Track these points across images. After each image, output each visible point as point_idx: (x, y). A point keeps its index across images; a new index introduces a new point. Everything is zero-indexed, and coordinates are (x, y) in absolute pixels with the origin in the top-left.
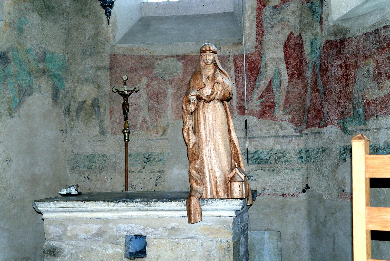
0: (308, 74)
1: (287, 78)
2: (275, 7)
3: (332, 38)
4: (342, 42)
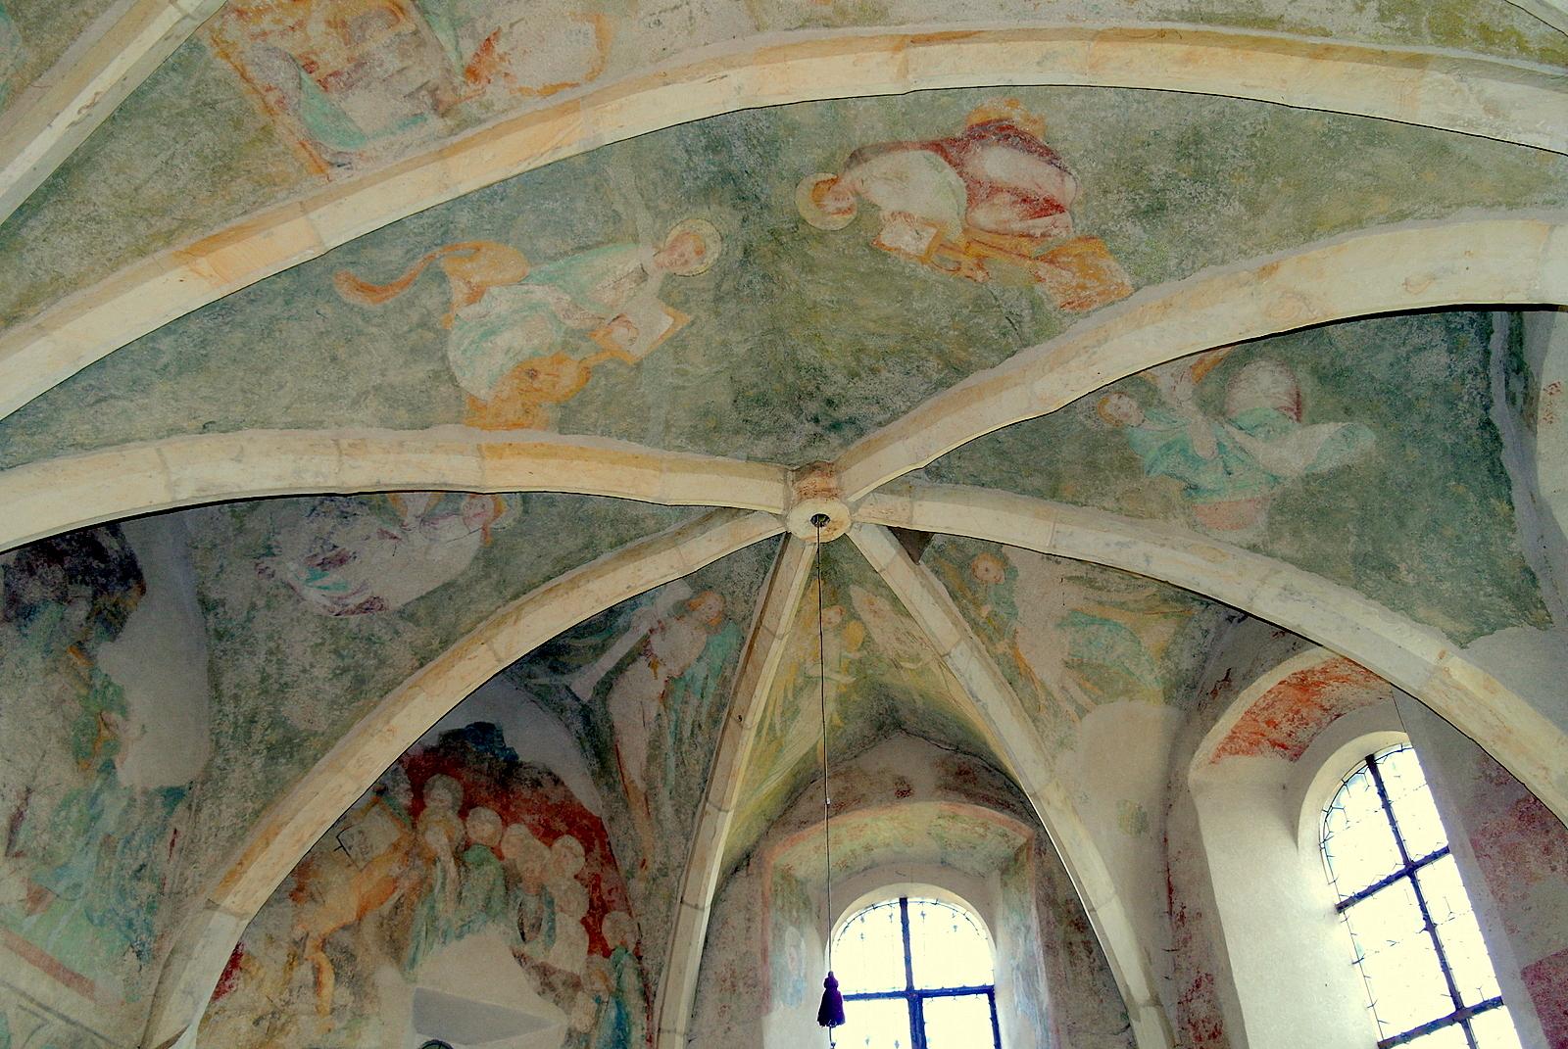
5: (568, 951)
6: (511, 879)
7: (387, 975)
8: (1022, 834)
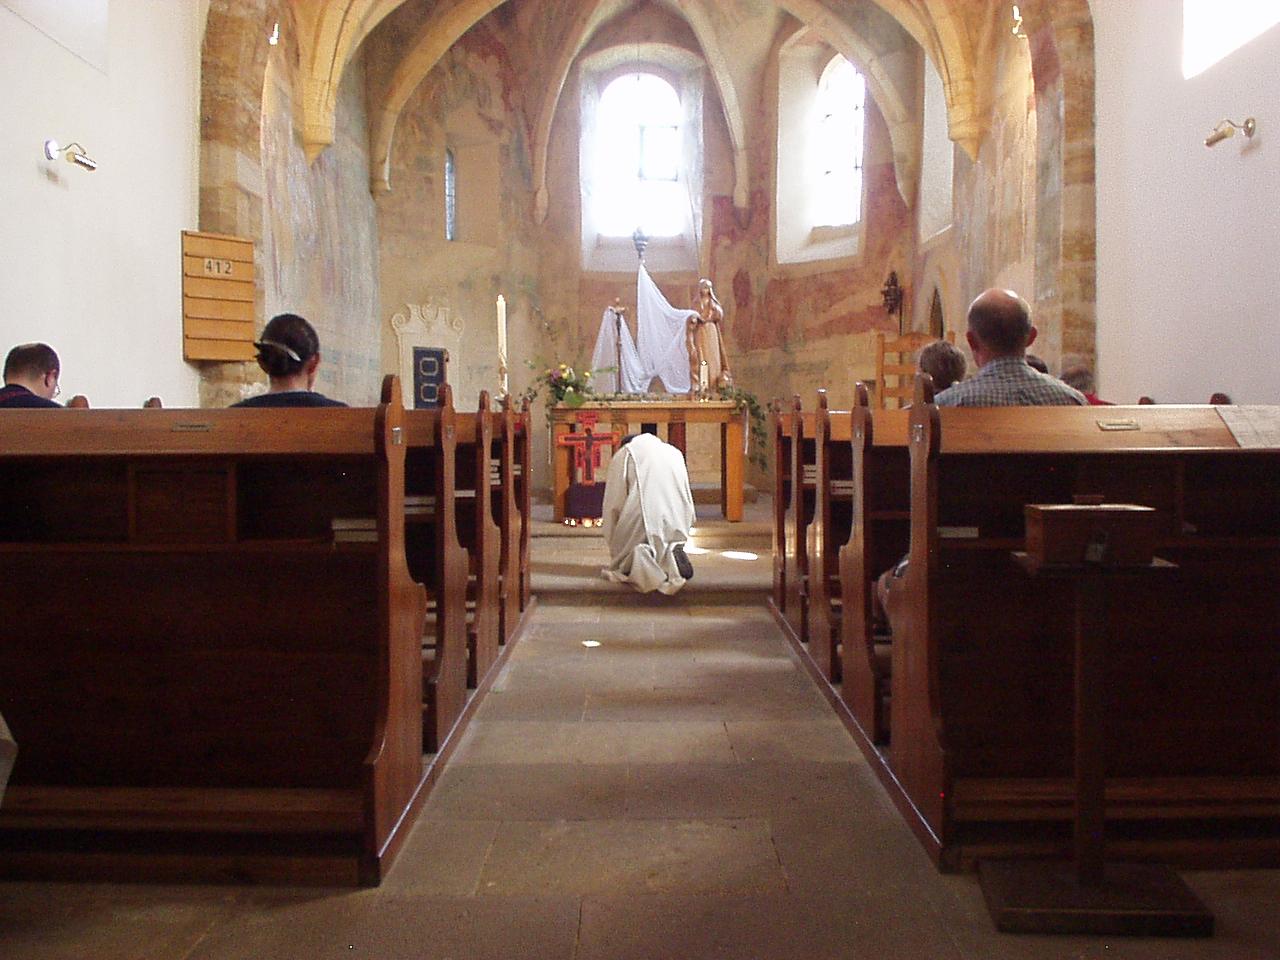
0: (754, 305)
1: (735, 307)
2: (726, 248)
3: (777, 278)
4: (786, 281)
5: (497, 111)
6: (473, 80)
7: (436, 127)
8: (701, 64)
